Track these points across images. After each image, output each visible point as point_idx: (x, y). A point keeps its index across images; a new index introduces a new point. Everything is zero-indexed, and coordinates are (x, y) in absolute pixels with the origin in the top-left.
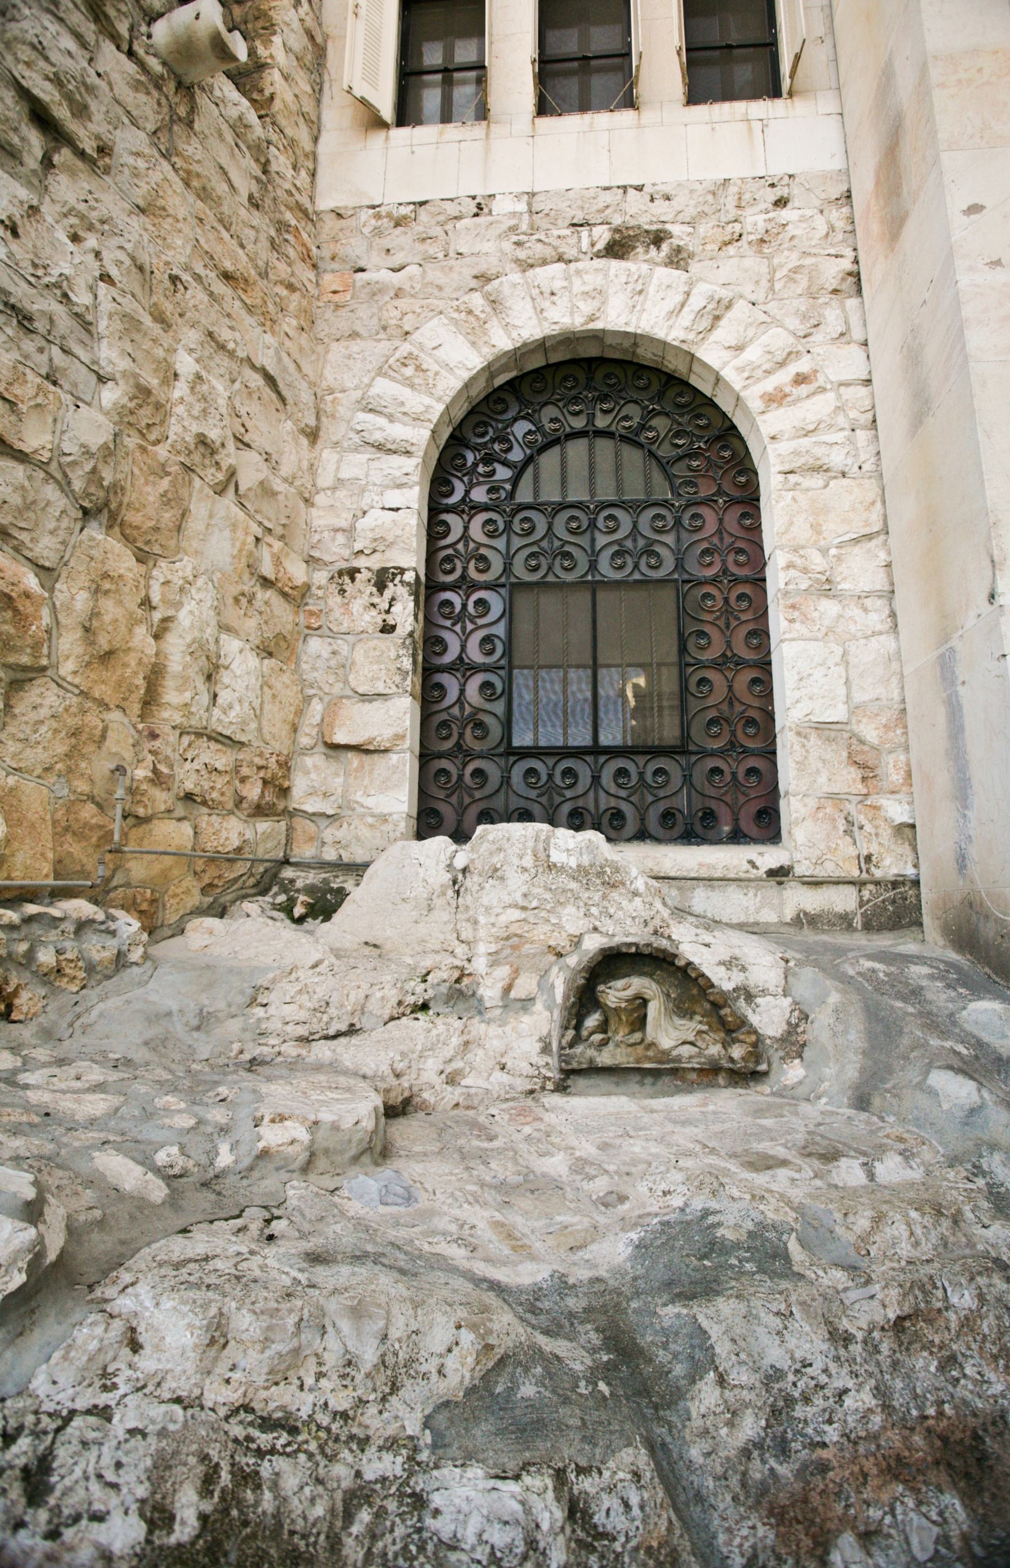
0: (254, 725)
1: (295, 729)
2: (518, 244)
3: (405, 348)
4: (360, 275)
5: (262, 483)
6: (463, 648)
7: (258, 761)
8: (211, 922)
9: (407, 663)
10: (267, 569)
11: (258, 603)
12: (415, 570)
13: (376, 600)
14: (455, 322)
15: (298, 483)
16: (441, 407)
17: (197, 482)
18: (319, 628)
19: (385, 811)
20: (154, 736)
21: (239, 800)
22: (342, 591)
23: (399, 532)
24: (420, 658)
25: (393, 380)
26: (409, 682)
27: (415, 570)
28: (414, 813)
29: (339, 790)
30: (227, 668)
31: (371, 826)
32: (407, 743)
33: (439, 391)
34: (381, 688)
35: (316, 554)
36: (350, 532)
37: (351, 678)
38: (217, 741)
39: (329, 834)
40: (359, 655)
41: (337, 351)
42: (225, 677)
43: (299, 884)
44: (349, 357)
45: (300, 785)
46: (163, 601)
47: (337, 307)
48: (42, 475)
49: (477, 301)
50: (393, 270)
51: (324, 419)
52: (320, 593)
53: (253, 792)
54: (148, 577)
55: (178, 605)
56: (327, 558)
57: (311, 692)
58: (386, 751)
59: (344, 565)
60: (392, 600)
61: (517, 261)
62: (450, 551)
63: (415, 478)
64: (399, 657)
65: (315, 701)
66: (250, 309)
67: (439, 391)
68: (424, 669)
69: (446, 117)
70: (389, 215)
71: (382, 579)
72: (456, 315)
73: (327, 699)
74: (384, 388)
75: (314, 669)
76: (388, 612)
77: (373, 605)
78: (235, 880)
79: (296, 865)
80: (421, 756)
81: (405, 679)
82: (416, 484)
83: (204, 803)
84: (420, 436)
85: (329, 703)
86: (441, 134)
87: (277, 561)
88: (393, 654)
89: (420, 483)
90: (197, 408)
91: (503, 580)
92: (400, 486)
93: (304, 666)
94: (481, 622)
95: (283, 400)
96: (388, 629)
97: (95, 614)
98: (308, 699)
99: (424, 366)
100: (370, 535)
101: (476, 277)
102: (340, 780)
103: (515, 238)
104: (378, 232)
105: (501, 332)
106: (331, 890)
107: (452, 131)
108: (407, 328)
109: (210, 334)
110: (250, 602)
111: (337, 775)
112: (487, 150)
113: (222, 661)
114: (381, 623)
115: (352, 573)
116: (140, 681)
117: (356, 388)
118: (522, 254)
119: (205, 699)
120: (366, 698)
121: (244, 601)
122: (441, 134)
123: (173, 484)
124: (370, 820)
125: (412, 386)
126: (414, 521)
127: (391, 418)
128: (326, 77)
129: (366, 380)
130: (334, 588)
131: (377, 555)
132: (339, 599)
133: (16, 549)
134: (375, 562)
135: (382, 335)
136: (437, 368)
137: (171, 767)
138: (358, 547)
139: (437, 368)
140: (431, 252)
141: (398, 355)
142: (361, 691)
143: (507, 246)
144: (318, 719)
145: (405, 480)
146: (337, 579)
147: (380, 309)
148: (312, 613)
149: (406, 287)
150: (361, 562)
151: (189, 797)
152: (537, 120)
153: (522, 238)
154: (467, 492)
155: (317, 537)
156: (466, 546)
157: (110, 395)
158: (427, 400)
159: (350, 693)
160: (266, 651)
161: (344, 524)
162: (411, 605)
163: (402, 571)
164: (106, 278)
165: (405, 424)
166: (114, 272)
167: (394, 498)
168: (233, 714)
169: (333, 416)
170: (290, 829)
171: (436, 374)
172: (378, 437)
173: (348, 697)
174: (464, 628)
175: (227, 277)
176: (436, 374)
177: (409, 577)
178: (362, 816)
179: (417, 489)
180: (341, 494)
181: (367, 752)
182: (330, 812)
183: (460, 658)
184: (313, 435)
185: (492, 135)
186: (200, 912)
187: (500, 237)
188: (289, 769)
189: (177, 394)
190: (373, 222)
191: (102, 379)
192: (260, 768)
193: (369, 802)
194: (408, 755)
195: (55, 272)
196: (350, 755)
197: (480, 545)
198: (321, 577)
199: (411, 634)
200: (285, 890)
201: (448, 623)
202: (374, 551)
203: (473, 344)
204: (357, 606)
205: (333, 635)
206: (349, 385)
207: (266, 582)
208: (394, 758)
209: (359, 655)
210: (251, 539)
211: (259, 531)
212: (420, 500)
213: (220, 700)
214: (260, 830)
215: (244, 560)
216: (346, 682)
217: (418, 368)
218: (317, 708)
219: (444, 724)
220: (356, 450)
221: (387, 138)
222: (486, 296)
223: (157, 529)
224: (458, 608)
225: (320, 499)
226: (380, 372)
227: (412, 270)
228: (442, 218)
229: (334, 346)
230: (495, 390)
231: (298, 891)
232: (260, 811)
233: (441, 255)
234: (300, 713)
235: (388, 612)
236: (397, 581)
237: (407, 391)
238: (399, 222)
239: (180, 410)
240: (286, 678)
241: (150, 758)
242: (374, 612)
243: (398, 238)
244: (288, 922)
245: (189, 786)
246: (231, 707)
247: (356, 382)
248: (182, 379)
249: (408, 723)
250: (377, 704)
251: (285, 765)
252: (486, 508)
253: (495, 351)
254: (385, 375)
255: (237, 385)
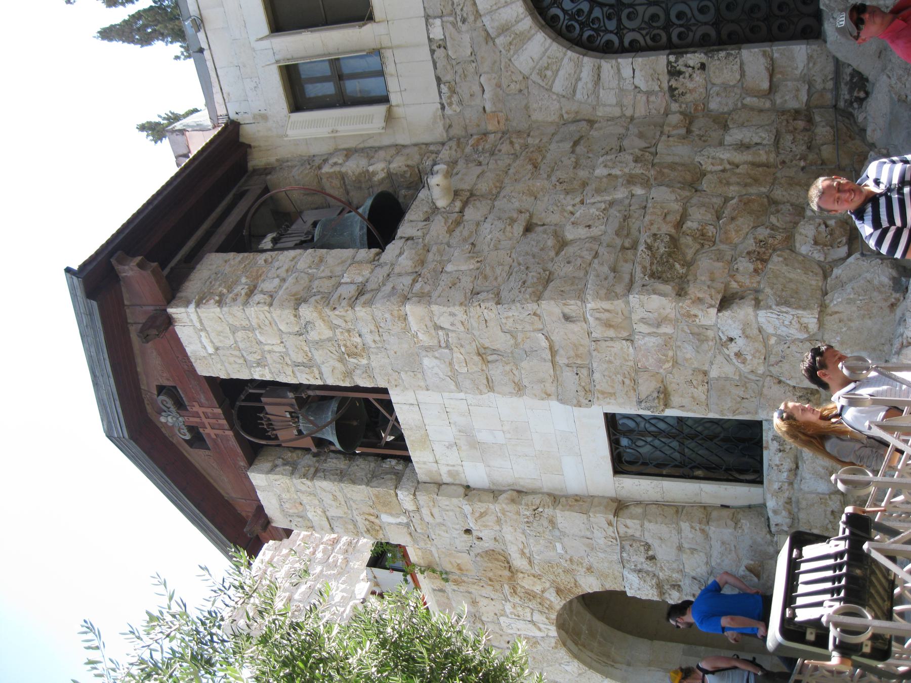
0: (767, 127)
1: (761, 111)
2: (464, 21)
3: (535, 77)
4: (487, 109)
5: (640, 138)
6: (706, 24)
7: (784, 123)
8: (869, 132)
9: (722, 54)
10: (683, 131)
11: (701, 133)
12: (668, 55)
13: (687, 75)
14: (516, 52)
15: (625, 124)
16: (569, 53)
17: (655, 161)
18: (703, 104)
19: (806, 57)
20: (784, 162)
21: (805, 130)
22: (683, 94)
23: (648, 66)
24: (715, 47)
25: (553, 82)
26: (733, 52)
27: (668, 55)
28: (805, 41)
29: (795, 83)
30: (741, 141)
31: (814, 64)
32: (768, 49)
33: (560, 55)
34: (736, 67)
35: (662, 111)
36: (649, 93)
37: (731, 84)
38: (778, 141)
39: (819, 86)
40: (718, 81)
41: (537, 116)
42: (746, 140)
43: (847, 97)
44: (541, 108)
45: (793, 104)
46: (721, 165)
47: (507, 120)
48: (688, 204)
49: (500, 41)
50: (484, 91)
51: (578, 118)
52: (684, 106)
53: (801, 124)
54: (711, 172)
55: (722, 160)
56: (664, 104)
57: (739, 105)
58: (772, 59)
59: (667, 95)
60: (687, 66)
61: (475, 21)
62: (648, 38)
63: (614, 62)
64: (719, 59)
65: (745, 102)
66: (544, 157)
67: (560, 55)
68: (720, 44)
69: (381, 73)
70: (450, 97)
71: (674, 73)
72: (512, 52)
73: (744, 95)
74: (558, 87)
75: (727, 105)
76: (693, 68)
77: (690, 76)
78: (847, 127)
79: (836, 101)
80: (770, 41)
81: (732, 54)
82: (617, 62)
83: (810, 142)
84: (588, 62)
85: (747, 94)
86: (392, 75)
87: (676, 127)
88: (718, 62)
89: (617, 59)
90: (624, 165)
91: (664, 5)
92: (619, 70)
93: (726, 110)
94: (690, 15)
95: (581, 138)
96: (703, 66)
97: (738, 184)
98: (744, 106)
99: (546, 65)
100: (650, 83)
101: (487, 43)
102: (789, 83)
103: (460, 24)
104: (461, 102)
105: (520, 24)
106: (851, 80)
107: (390, 69)
108: (521, 78)
109: (574, 168)
110: (703, 136)
111: (786, 85)
112: (399, 47)
113: (739, 143)
114: (700, 71)
115: (672, 89)
116: (760, 169)
117: (559, 102)
118: (471, 18)
119: (760, 147)
120: (743, 74)
121: (703, 139)
122: (392, 75)
123: (665, 168)
124: (811, 65)
125: (558, 71)
126: (640, 60)
127: (579, 79)
128: (362, 146)
129: (555, 97)
130: (681, 99)
131: (660, 77)
132: (688, 95)
133: (722, 208)
134: (665, 78)
135: (525, 92)
136: (545, 59)
137: (797, 155)
138: (657, 88)
139: (545, 59)
140: (473, 70)
141: (540, 82)
142: (739, 77)
143: (464, 28)
144: (755, 99)
145: (615, 68)
146: (676, 98)
147: (508, 95)
148: (696, 109)
149: (494, 82)
150: (665, 86)
151: (809, 148)
152: (377, 20)
153: (459, 20)
154: (611, 32)
155: (653, 111)
156: (644, 29)
157: (639, 191)
158: (566, 60)
159: (740, 83)
160: (726, 127)
161: (644, 98)
162: (689, 55)
163: (669, 63)
164: (582, 202)
165: (581, 72)
166: (578, 200)
167: (627, 72)
168: (763, 135)
169: (577, 113)
170: (816, 107)
171: (549, 57)
172: (590, 86)
173: (742, 84)
174: (694, 25)
175: (536, 167)
176: (549, 57)
177: (672, 58)
178: (809, 69)
179: (619, 60)
180: (625, 102)
181: (773, 70)
182: (807, 87)
183: (712, 25)
184: (591, 122)
185: (390, 45)
186: (864, 139)
187: (459, 31)
188: (783, 111)
189: (619, 173)
190: (454, 106)
191: (633, 195)
192: (788, 122)
193: (801, 66)
194: (775, 48)
195: (597, 213)
196: (775, 80)
197: (643, 21)
198: (675, 107)
199: (706, 54)
200: (851, 103)
201: (691, 34)
202: (658, 79)
203: (529, 39)
204: (690, 85)
205: (708, 96)
206: (558, 106)
207: (689, 131)
208: (776, 55)
209: (718, 81)
210: (671, 139)
211: (664, 138)
212: (625, 57)
213: (759, 141)
214: (820, 120)
215: (683, 141)
216: (734, 86)
217: (547, 68)
218: (748, 100)
219: (752, 30)
220: (598, 97)
221: (397, 106)
222: (499, 35)
223: (689, 171)
224: (682, 29)
225: (629, 113)
226: (549, 90)
227: (483, 80)
228: (449, 67)
229: (534, 117)
230: (547, 23)
231: (852, 96)
232: (810, 120)
233: (474, 65)
234: (752, 109)
235: (693, 68)
236: (675, 65)
237: (561, 73)
238: (453, 91)
239: (627, 170)
240: (736, 117)
241: (794, 162)
242: (695, 75)
243: (464, 89)
244: (869, 99)
245: (804, 148)
246: (761, 137)
247: (555, 102)
248: (610, 172)
249: (756, 50)
250: (746, 68)
251: (783, 112)
252: (619, 20)
253: (533, 26)
254: (551, 87)
255: (590, 155)
